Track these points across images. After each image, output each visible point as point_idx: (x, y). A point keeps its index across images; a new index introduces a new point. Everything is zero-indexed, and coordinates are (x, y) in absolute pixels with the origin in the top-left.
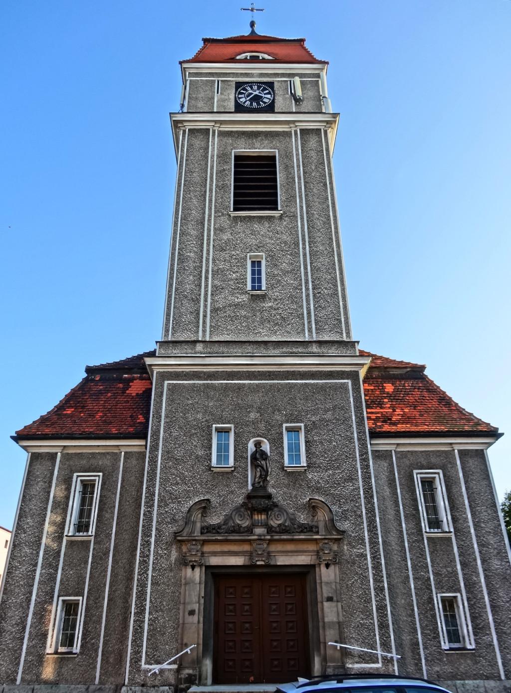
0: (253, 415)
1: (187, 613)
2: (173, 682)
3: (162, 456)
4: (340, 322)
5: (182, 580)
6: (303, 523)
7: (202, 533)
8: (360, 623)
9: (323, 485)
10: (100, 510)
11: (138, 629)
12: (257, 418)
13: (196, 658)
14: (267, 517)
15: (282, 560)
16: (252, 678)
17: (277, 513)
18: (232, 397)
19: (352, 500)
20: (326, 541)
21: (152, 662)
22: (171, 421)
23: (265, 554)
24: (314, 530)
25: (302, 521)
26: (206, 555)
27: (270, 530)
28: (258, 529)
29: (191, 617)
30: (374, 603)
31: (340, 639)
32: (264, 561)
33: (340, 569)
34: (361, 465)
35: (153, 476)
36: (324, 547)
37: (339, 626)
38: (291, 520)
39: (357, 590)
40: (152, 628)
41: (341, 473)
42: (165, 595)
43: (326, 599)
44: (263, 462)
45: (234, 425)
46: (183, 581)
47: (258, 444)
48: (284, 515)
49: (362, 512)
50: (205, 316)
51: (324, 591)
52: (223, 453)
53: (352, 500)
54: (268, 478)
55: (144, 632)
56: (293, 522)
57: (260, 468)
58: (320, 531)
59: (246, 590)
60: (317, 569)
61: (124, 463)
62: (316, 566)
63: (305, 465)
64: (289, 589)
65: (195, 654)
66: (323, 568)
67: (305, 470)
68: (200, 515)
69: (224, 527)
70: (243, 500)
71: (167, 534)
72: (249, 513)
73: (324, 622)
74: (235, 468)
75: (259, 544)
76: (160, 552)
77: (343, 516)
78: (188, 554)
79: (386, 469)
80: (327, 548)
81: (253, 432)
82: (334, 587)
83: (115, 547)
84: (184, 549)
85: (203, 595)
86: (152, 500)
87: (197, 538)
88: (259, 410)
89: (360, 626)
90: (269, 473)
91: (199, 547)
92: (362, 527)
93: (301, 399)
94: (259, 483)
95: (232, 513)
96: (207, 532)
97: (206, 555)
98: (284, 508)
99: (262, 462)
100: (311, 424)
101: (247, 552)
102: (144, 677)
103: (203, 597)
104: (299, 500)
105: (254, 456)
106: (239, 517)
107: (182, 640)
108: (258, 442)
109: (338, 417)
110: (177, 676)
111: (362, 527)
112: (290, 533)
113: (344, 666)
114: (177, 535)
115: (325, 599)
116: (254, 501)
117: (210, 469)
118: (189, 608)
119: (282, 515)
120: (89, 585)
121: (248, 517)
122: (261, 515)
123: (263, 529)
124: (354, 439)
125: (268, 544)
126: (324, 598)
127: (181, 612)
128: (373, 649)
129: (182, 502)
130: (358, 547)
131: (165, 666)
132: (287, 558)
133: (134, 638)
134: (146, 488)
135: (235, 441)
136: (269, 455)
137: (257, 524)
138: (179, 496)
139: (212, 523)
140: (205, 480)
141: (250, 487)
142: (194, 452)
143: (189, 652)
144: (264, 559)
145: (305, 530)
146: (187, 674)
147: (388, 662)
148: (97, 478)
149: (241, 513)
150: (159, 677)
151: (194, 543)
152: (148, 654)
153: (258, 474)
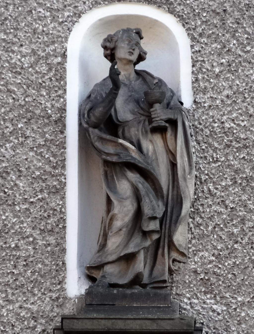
44: (154, 146)
54: (180, 236)
57: (133, 176)
90: (186, 207)
94: (129, 258)
99: (146, 145)
105: (99, 111)
108: (127, 31)
136: (187, 99)
141: (75, 286)
153: (124, 211)
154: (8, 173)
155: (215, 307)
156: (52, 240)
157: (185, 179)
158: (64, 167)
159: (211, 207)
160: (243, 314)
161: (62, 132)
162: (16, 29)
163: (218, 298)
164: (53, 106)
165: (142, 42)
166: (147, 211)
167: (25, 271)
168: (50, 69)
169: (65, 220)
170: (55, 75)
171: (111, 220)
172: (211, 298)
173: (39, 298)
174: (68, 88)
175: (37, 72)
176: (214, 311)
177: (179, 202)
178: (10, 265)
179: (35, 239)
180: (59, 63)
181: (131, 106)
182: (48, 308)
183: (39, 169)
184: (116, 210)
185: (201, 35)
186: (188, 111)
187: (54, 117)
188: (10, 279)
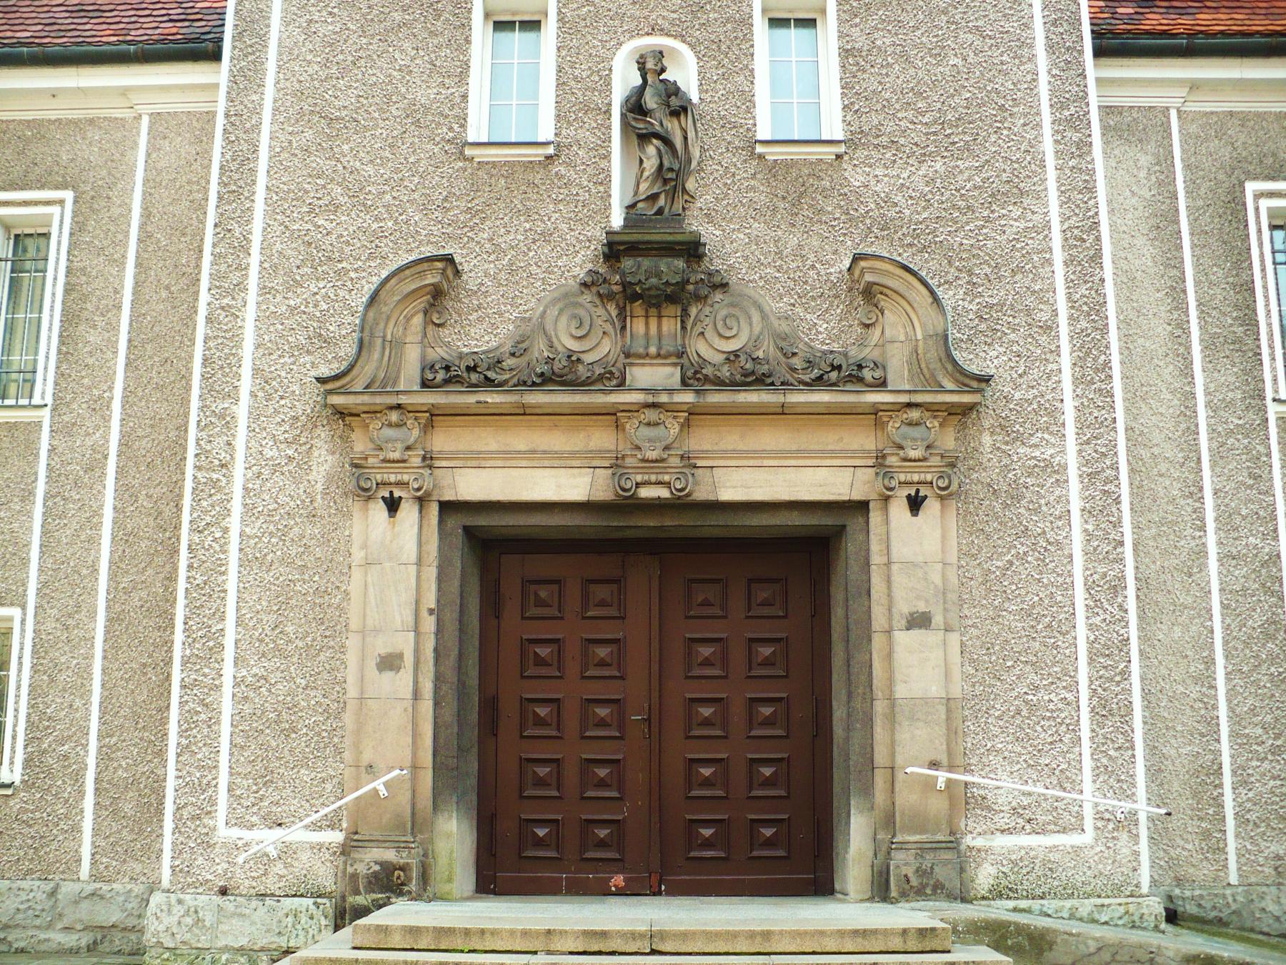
1: (372, 664)
2: (329, 884)
3: (275, 110)
5: (354, 550)
6: (824, 353)
7: (425, 384)
8: (1026, 702)
9: (907, 212)
10: (70, 318)
11: (198, 713)
13: (409, 812)
14: (683, 328)
16: (619, 880)
17: (724, 312)
19: (1020, 269)
20: (915, 414)
21: (254, 819)
23: (675, 461)
25: (823, 343)
26: (444, 464)
27: (695, 377)
28: (647, 369)
29: (388, 675)
30: (1082, 632)
31: (950, 753)
32: (667, 485)
33: (963, 515)
34: (1056, 142)
35: (241, 183)
37: (949, 711)
39: (1023, 592)
40: (248, 709)
41: (979, 169)
42: (293, 602)
43: (904, 622)
44: (672, 127)
46: (358, 555)
47: (651, 65)
49: (1055, 313)
51: (899, 593)
52: (513, 93)
53: (1020, 269)
54: (691, 185)
55: (218, 722)
56: (783, 344)
57: (655, 141)
58: (890, 377)
59: (601, 592)
60: (875, 517)
61: (148, 155)
62: (871, 505)
63: (839, 136)
64: (763, 594)
65: (404, 798)
66: (899, 508)
67: (839, 157)
68: (418, 320)
69: (510, 362)
70: (590, 266)
71: (296, 388)
72: (614, 313)
73: (892, 701)
75: (649, 424)
76: (269, 453)
77: (983, 326)
78: (371, 460)
79: (1142, 174)
80: (914, 439)
81: (632, 17)
82: (937, 579)
83: (124, 444)
84: (360, 444)
85: (433, 606)
86: (239, 268)
87: (403, 399)
89: (1024, 713)
90: (694, 164)
91: (416, 432)
92: (1055, 367)
95: (544, 312)
96: (447, 382)
97: (444, 464)
98: (752, 293)
101: (600, 453)
102: (226, 866)
103: (431, 611)
104: (813, 267)
106: (574, 323)
107: (357, 747)
110: (341, 867)
111: (1055, 367)
112: (772, 384)
113: (958, 842)
114: (329, 386)
115: (899, 622)
116: (628, 263)
117: (462, 153)
118: (382, 646)
120: (41, 570)
121: (609, 328)
122: (660, 317)
123: (669, 369)
124: (1031, 46)
125: (686, 425)
126: (896, 616)
127: (352, 658)
128: (1068, 786)
129: (353, 275)
130: (1034, 440)
131: (297, 834)
132: (761, 475)
133: (184, 742)
134: (216, 225)
135: (558, 49)
137: (641, 350)
138: (341, 251)
139: (465, 350)
140: (438, 197)
142: (399, 93)
143: (383, 792)
144: (667, 478)
145: (834, 375)
146: (376, 863)
147: (1116, 829)
148: (55, 210)
149: (582, 312)
150: (279, 868)
151: (394, 416)
152: (238, 792)
153: (651, 165)
156: (602, 189)
159: (710, 166)
166: (666, 164)
177: (690, 161)
181: (656, 99)
184: (646, 164)
188: (572, 215)
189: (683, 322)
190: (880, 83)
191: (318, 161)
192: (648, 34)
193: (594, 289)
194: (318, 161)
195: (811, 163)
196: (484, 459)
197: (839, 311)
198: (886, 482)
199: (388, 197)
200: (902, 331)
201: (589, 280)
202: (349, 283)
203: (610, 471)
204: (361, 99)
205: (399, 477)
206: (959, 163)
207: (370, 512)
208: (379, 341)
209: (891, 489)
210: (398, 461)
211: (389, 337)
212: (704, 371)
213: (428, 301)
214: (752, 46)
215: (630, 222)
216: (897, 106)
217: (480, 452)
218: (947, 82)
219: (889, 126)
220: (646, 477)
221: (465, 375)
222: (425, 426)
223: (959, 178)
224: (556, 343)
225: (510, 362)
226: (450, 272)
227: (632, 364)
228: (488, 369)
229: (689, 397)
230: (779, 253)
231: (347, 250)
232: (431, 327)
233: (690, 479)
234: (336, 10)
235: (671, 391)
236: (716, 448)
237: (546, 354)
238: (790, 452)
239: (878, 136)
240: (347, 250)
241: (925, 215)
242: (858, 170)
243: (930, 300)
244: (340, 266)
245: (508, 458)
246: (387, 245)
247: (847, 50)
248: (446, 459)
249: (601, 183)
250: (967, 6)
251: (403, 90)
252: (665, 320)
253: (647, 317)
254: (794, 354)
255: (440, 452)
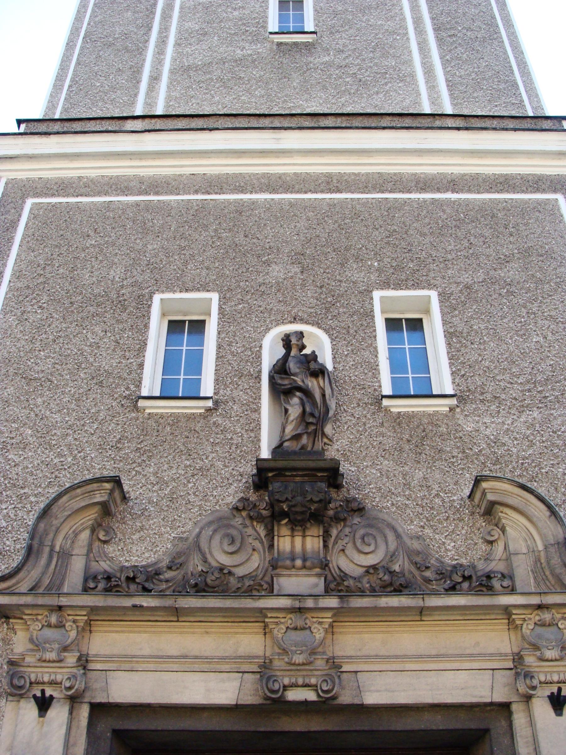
0: (277, 272)
4: (515, 85)
6: (454, 567)
9: (514, 450)
12: (292, 277)
14: (325, 546)
15: (382, 689)
17: (362, 532)
18: (216, 230)
20: (547, 616)
22: (28, 287)
23: (320, 663)
24: (496, 584)
26: (99, 666)
27: (337, 585)
28: (293, 580)
32: (314, 687)
36: (539, 637)
38: (410, 553)
45: (220, 292)
48: (386, 537)
50: (155, 79)
54: (328, 429)
56: (418, 559)
60: (519, 718)
68: (85, 535)
69: (169, 575)
74: (216, 403)
75: (296, 629)
88: (297, 258)
90: (331, 413)
91: (73, 634)
93: (423, 235)
95: (200, 533)
98: (386, 517)
100: (461, 291)
101: (249, 658)
106: (226, 542)
109: (538, 275)
119: (380, 540)
121: (257, 544)
122: (304, 536)
123: (314, 580)
129: (33, 499)
135: (219, 333)
136: (330, 366)
138: (26, 480)
140: (112, 439)
141: (265, 454)
144: (313, 681)
149: (234, 532)
154: (228, 402)
155: (350, 468)
156: (252, 435)
157: (330, 400)
158: (260, 399)
159: (345, 417)
160: (368, 472)
161: (259, 383)
162: (235, 336)
163: (352, 464)
164: (254, 370)
165: (304, 339)
166: (308, 409)
167: (236, 451)
168: (253, 354)
169: (260, 425)
170: (255, 356)
171: (287, 419)
172: (348, 464)
173: (244, 465)
174: (263, 362)
175: (245, 355)
176: (350, 470)
177: (327, 411)
178: (227, 448)
179: (242, 434)
180: (257, 351)
182: (250, 470)
183: (245, 400)
185: (336, 338)
186: (331, 372)
187: (255, 375)
189: (325, 541)
190: (479, 355)
191: (15, 410)
192: (291, 322)
193: (244, 514)
194: (15, 410)
195: (429, 415)
196: (137, 662)
197: (464, 532)
198: (528, 681)
199: (70, 438)
200: (523, 544)
201: (240, 505)
202: (28, 506)
203: (258, 676)
204: (56, 366)
205: (53, 677)
206: (552, 412)
207: (21, 712)
208: (47, 550)
209: (534, 688)
210: (54, 661)
211: (57, 548)
212: (346, 583)
213: (95, 519)
214: (375, 331)
215: (278, 450)
216: (496, 371)
217: (134, 657)
218: (534, 353)
219: (491, 387)
220: (293, 680)
221: (124, 585)
222: (83, 629)
223: (555, 422)
224: (210, 559)
225: (169, 575)
226: (117, 494)
227: (279, 575)
228: (146, 581)
229: (333, 602)
230: (407, 485)
231: (30, 479)
232: (97, 544)
233: (337, 681)
234: (45, 305)
235: (315, 596)
236: (359, 654)
237: (200, 568)
238: (429, 656)
239: (482, 393)
240: (30, 479)
241: (531, 452)
242: (469, 419)
243: (548, 513)
244: (22, 491)
245: (161, 661)
246: (65, 476)
247: (451, 333)
248: (101, 662)
249: (252, 431)
250: (541, 302)
251: (92, 360)
252: (308, 539)
253: (293, 536)
254: (427, 568)
255: (96, 656)
